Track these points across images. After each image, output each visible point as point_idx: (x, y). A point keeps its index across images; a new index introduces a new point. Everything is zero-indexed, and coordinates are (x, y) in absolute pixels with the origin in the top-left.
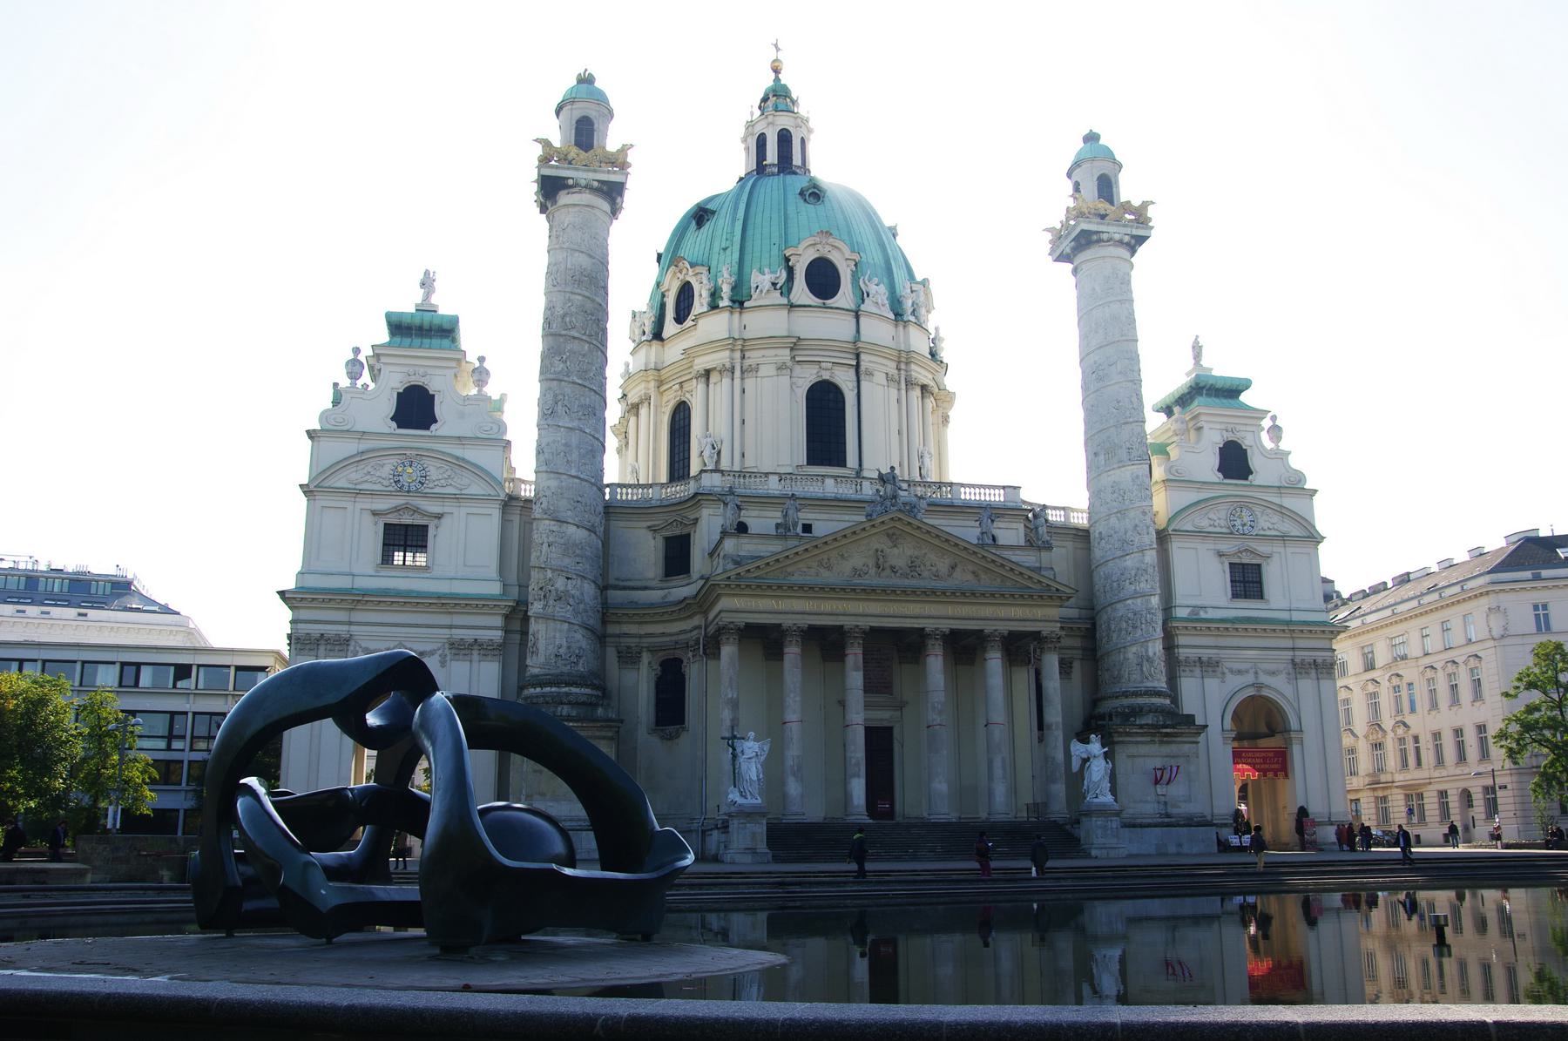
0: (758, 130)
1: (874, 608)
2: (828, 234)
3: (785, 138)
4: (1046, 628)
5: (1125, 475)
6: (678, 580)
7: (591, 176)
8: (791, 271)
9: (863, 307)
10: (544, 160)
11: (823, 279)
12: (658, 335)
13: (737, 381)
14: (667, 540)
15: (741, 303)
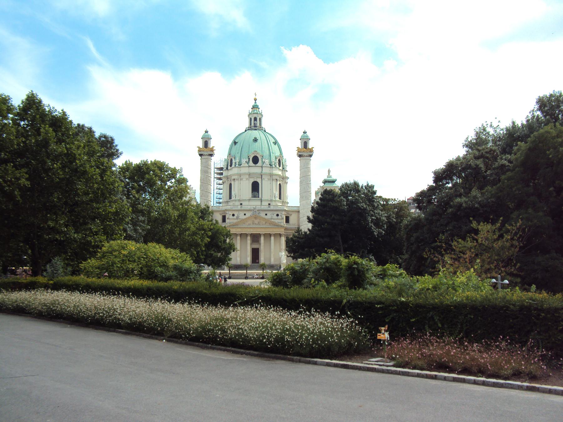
0: (251, 116)
1: (252, 230)
2: (256, 151)
3: (255, 119)
4: (281, 233)
5: (304, 202)
6: (224, 223)
7: (207, 153)
8: (249, 159)
9: (263, 165)
10: (199, 151)
11: (255, 160)
12: (227, 168)
13: (239, 181)
14: (223, 216)
15: (240, 165)
